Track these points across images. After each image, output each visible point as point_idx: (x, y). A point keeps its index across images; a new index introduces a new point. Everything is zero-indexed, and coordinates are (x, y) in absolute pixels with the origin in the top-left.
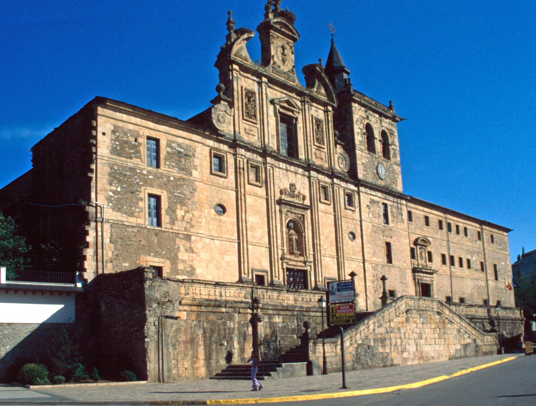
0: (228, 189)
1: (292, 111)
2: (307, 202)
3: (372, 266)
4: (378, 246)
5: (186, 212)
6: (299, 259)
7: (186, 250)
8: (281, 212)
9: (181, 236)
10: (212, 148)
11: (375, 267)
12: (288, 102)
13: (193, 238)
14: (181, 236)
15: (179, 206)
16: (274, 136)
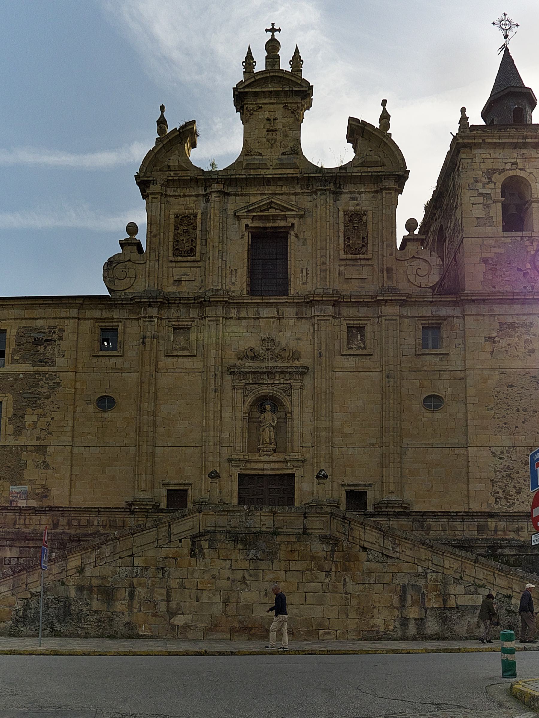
0: (122, 373)
1: (285, 218)
2: (305, 361)
3: (492, 453)
4: (518, 410)
5: (40, 416)
6: (271, 458)
7: (36, 466)
8: (234, 388)
9: (29, 448)
10: (96, 320)
11: (502, 452)
12: (270, 205)
13: (50, 449)
14: (29, 448)
15: (29, 410)
16: (236, 270)
